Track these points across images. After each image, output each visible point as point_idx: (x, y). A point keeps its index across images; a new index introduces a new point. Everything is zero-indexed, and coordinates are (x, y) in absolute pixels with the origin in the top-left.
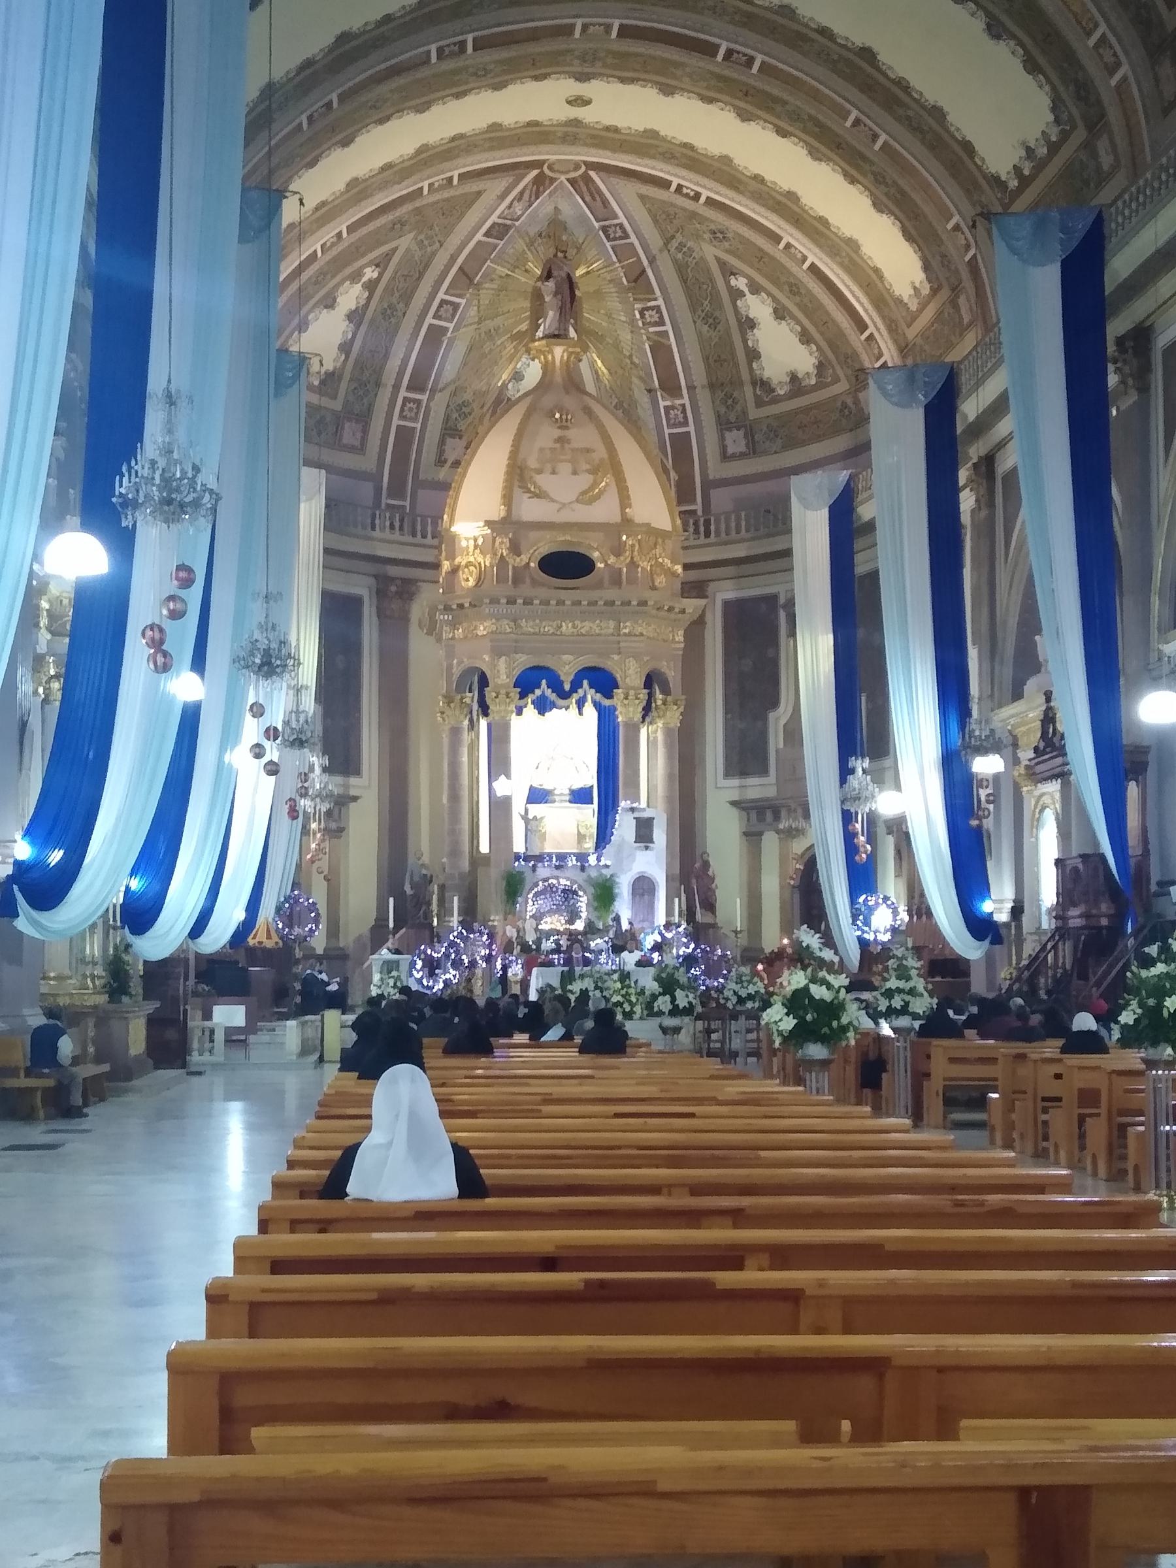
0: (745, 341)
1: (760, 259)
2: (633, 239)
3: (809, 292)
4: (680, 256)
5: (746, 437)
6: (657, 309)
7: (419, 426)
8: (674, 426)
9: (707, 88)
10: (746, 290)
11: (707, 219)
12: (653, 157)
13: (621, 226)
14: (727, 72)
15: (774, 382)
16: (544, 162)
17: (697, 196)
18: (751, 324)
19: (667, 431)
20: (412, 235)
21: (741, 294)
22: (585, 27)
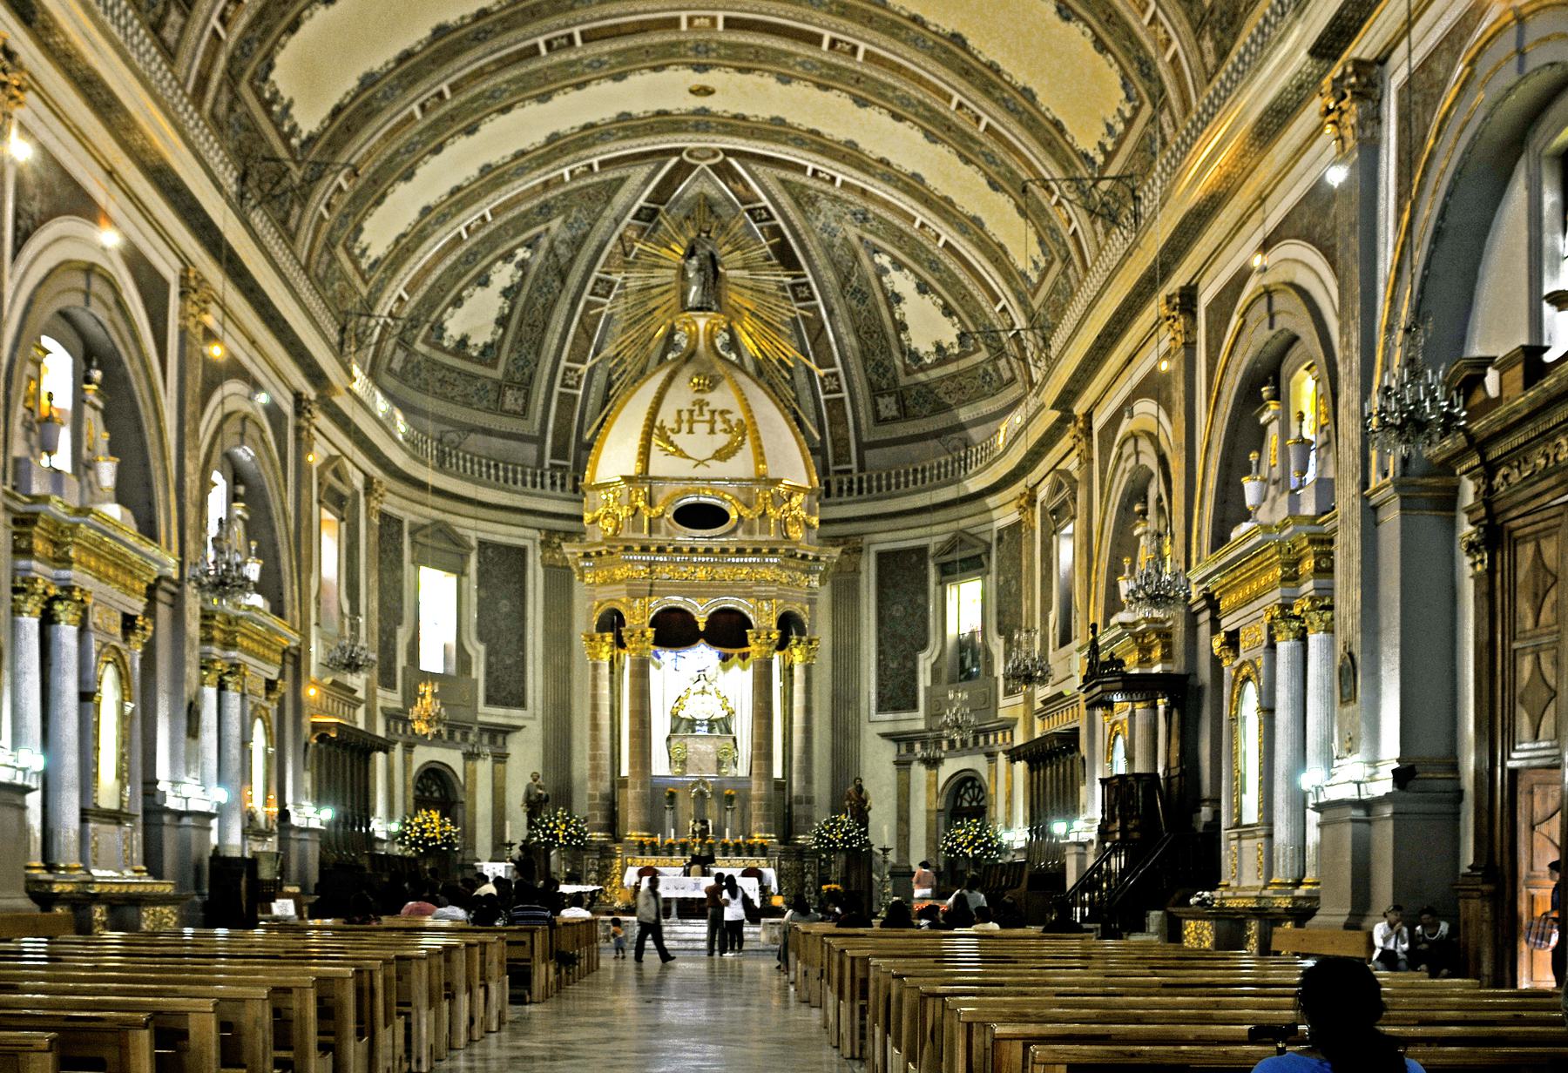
0: (892, 315)
1: (900, 237)
2: (779, 221)
3: (947, 269)
4: (825, 236)
5: (897, 402)
6: (807, 285)
7: (580, 393)
8: (830, 392)
9: (821, 76)
10: (889, 267)
11: (847, 201)
12: (785, 143)
13: (766, 209)
14: (834, 60)
15: (922, 352)
16: (682, 149)
17: (833, 179)
18: (898, 298)
19: (822, 397)
20: (561, 218)
21: (886, 271)
22: (690, 20)
